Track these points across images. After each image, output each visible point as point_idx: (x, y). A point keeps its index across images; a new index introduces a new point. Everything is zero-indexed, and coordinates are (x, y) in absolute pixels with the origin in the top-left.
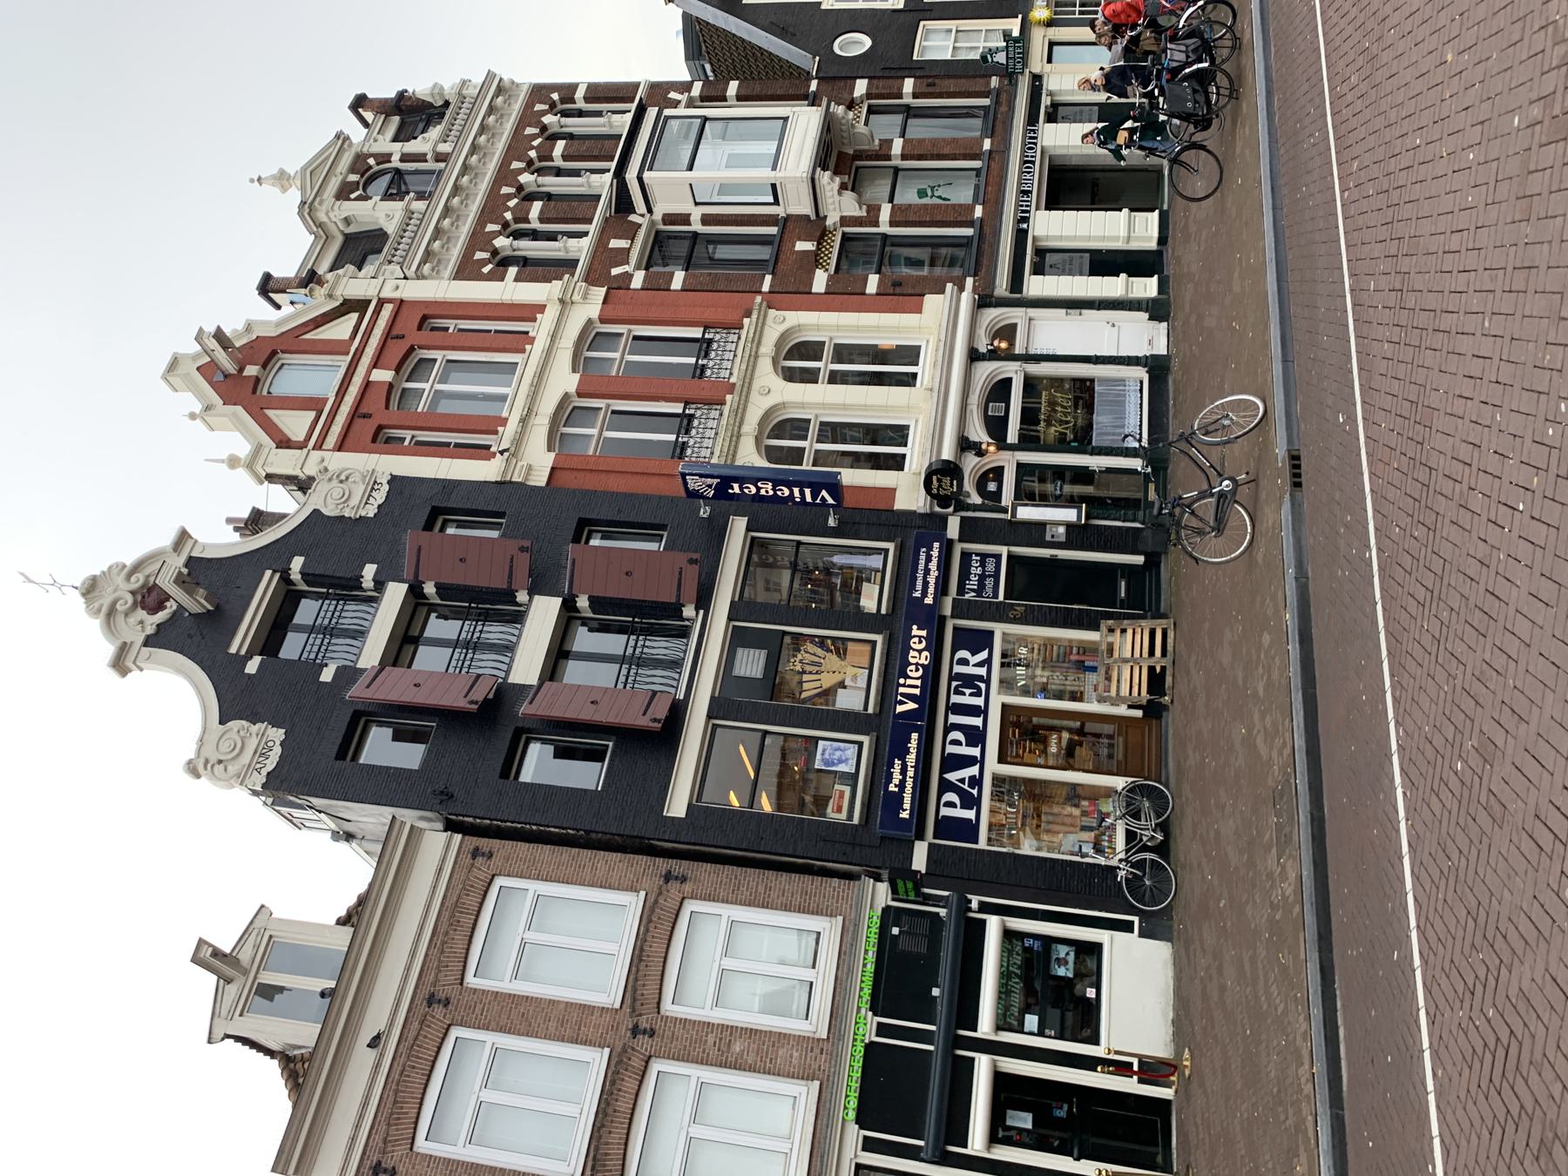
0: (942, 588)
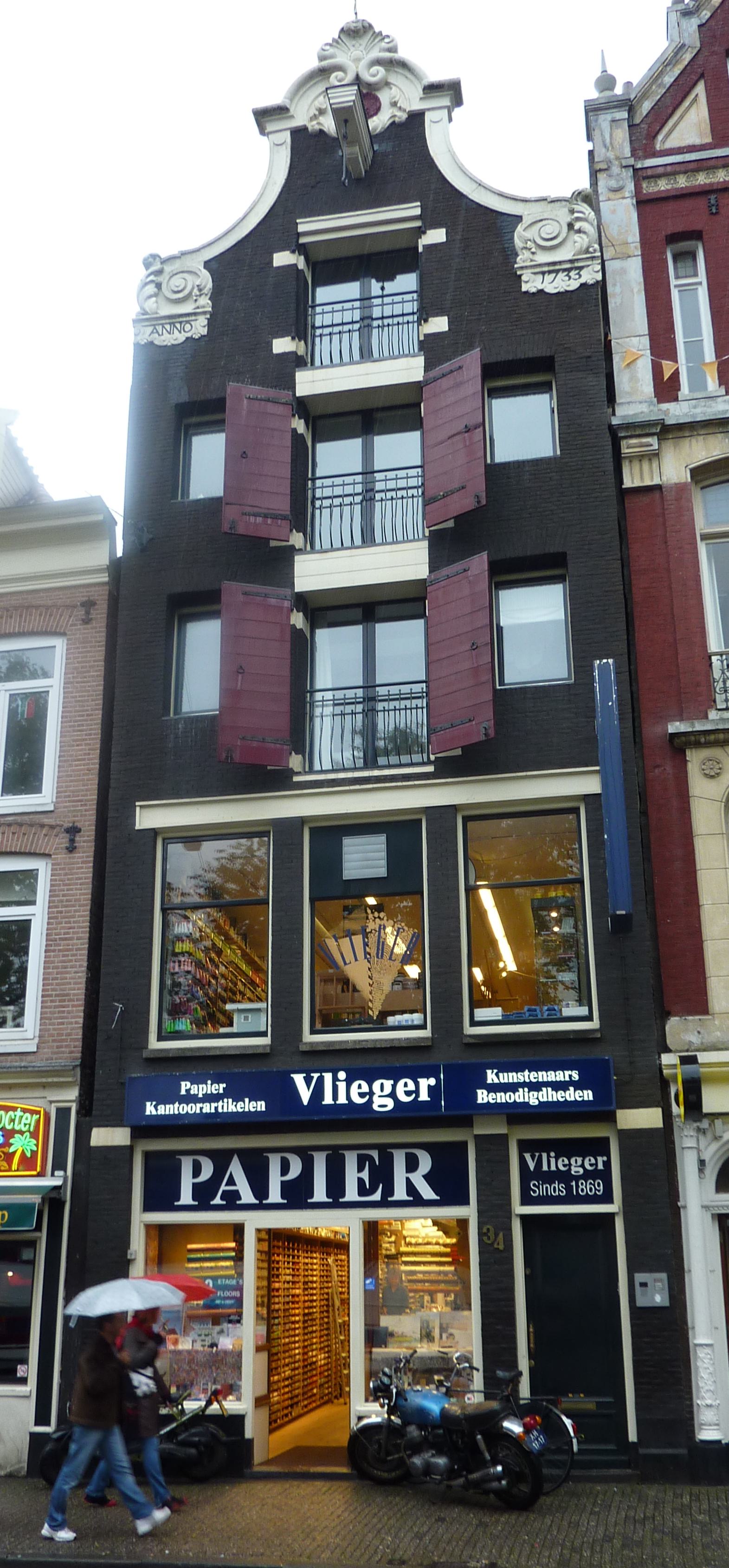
0: (519, 1115)
